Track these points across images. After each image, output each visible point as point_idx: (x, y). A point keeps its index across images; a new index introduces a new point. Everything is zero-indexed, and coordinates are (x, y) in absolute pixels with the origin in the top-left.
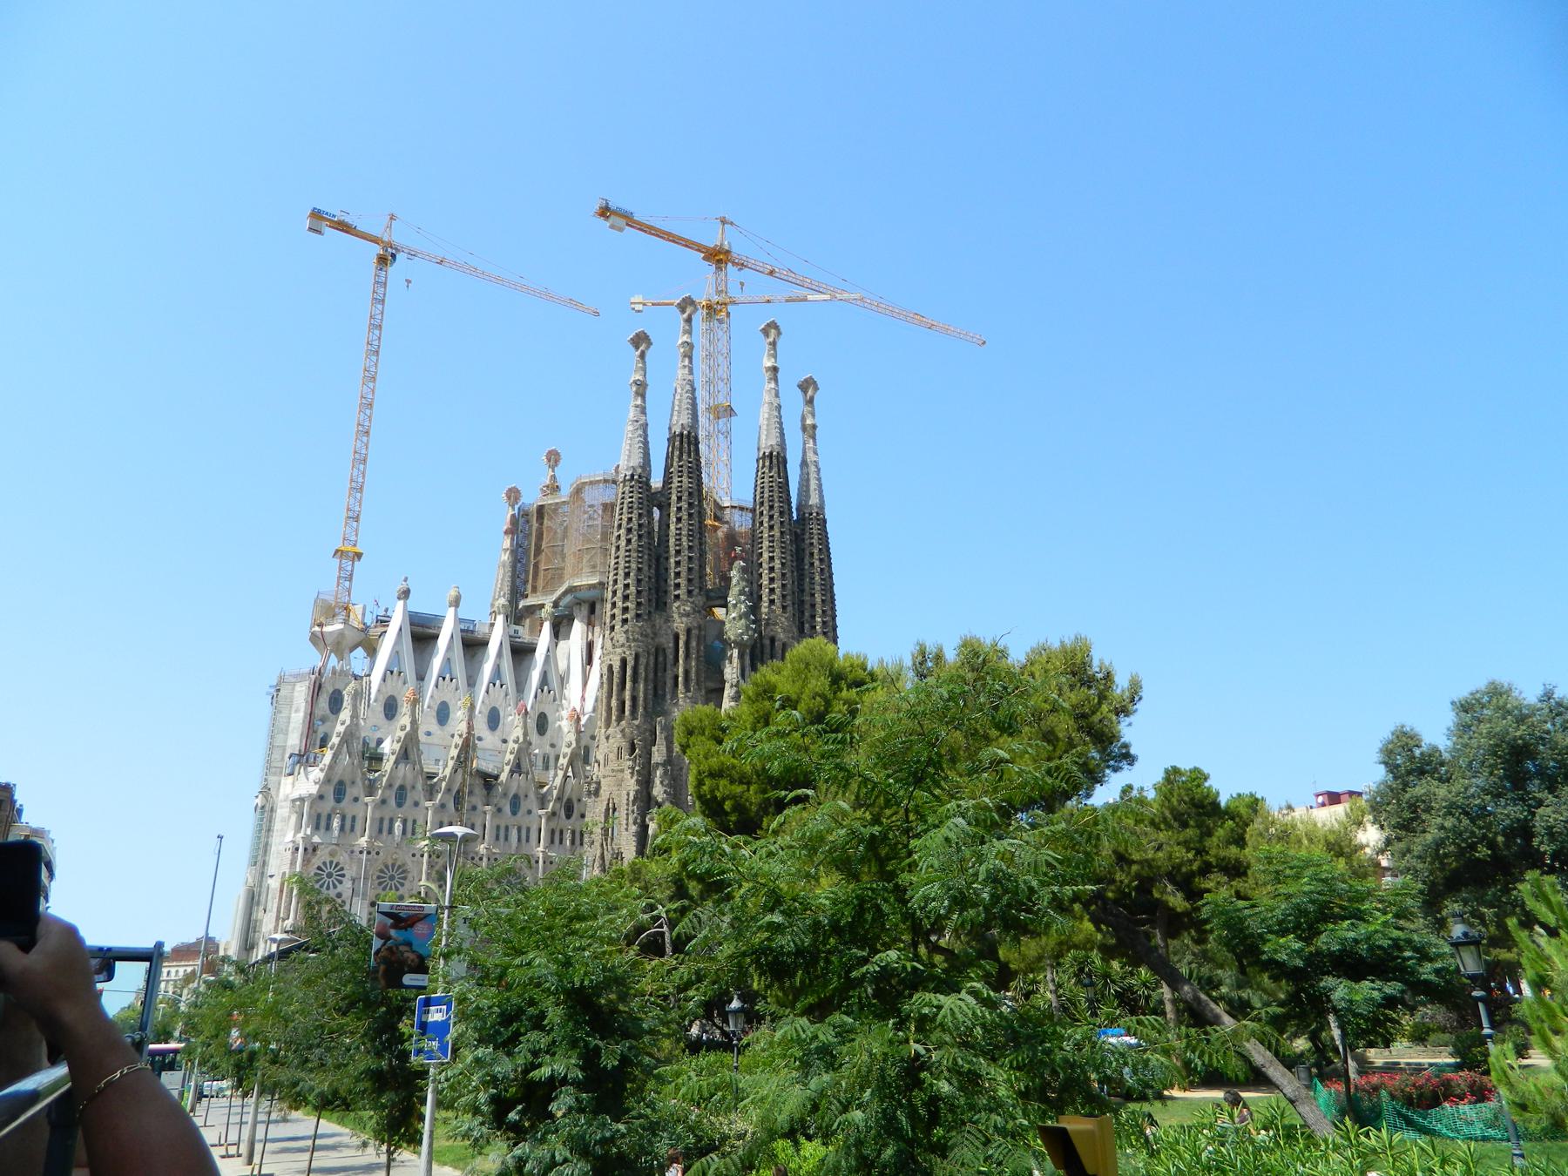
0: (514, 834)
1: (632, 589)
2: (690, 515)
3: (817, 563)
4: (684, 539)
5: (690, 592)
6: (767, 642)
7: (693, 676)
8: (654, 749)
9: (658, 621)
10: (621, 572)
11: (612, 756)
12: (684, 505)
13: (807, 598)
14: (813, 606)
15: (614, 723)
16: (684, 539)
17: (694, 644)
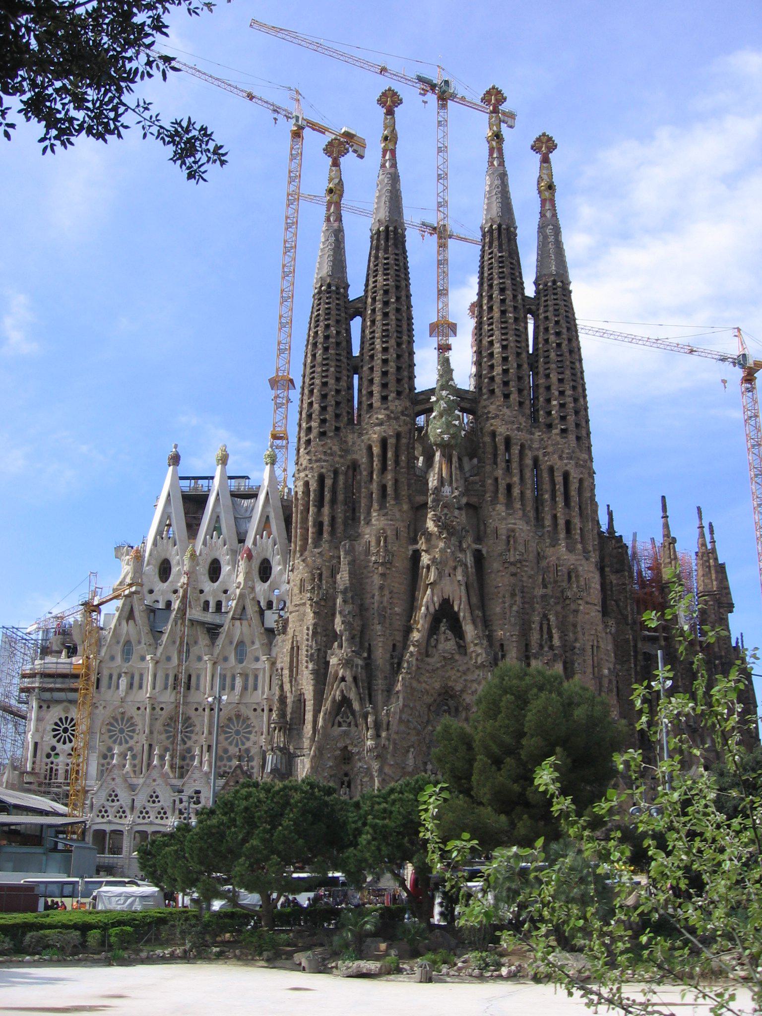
0: (239, 682)
1: (316, 406)
2: (386, 315)
3: (552, 338)
4: (378, 341)
5: (384, 398)
6: (487, 439)
7: (390, 490)
8: (338, 577)
9: (351, 438)
10: (306, 391)
11: (296, 590)
12: (379, 305)
13: (542, 381)
14: (548, 388)
15: (298, 555)
16: (378, 341)
17: (390, 454)
